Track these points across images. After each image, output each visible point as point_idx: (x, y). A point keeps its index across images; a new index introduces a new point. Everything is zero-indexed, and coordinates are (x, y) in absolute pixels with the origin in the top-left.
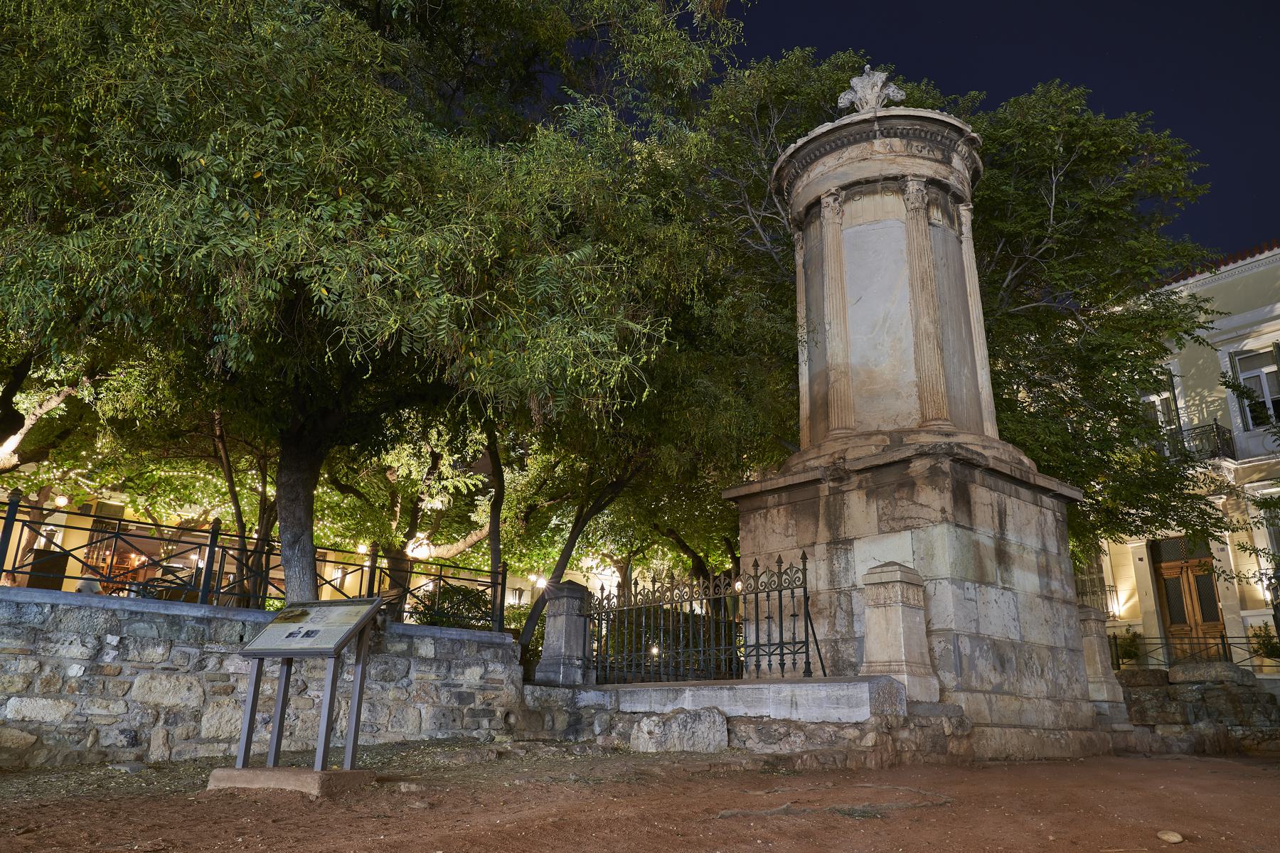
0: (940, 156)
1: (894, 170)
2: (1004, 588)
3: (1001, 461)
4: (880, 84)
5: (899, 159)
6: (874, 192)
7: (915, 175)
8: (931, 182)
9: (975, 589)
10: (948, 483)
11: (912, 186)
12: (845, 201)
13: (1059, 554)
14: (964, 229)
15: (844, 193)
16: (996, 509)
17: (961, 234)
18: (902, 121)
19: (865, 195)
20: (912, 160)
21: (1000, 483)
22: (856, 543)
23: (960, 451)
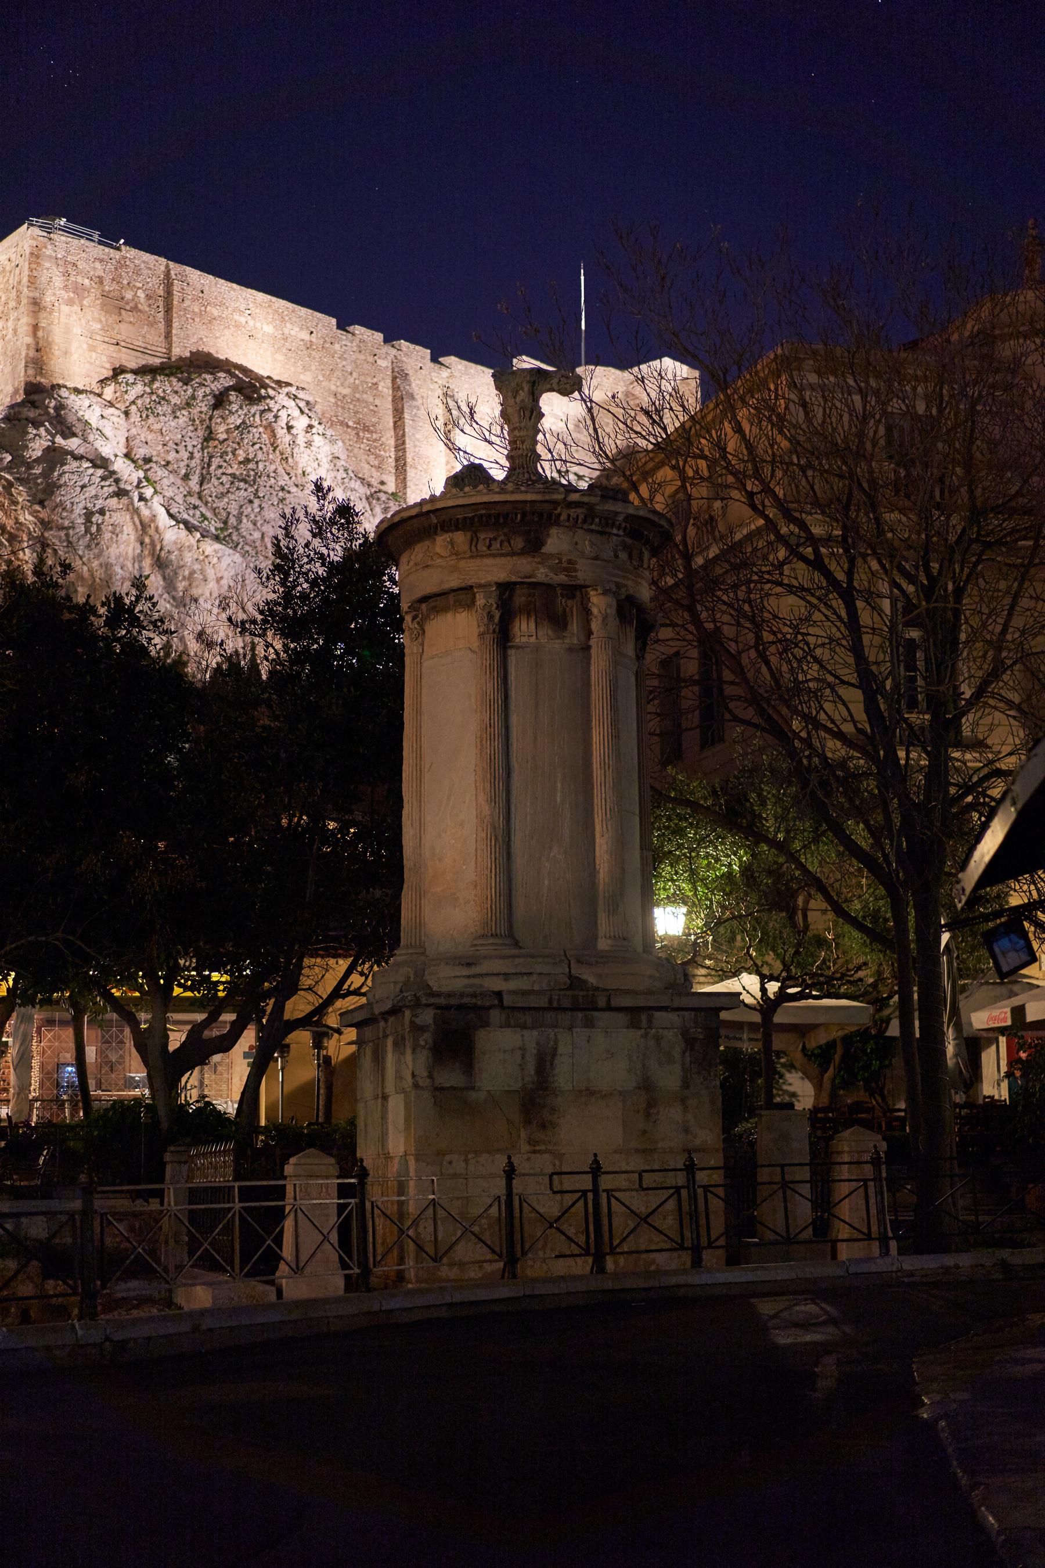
0: (519, 543)
1: (454, 582)
2: (534, 1152)
3: (525, 993)
4: (526, 387)
5: (462, 564)
6: (446, 609)
7: (480, 586)
8: (505, 589)
9: (466, 1161)
10: (426, 1038)
11: (480, 601)
12: (426, 618)
13: (686, 1085)
14: (595, 626)
15: (424, 606)
16: (532, 1051)
17: (589, 633)
18: (459, 509)
19: (437, 612)
20: (479, 560)
21: (549, 1016)
22: (390, 1099)
23: (432, 1000)
